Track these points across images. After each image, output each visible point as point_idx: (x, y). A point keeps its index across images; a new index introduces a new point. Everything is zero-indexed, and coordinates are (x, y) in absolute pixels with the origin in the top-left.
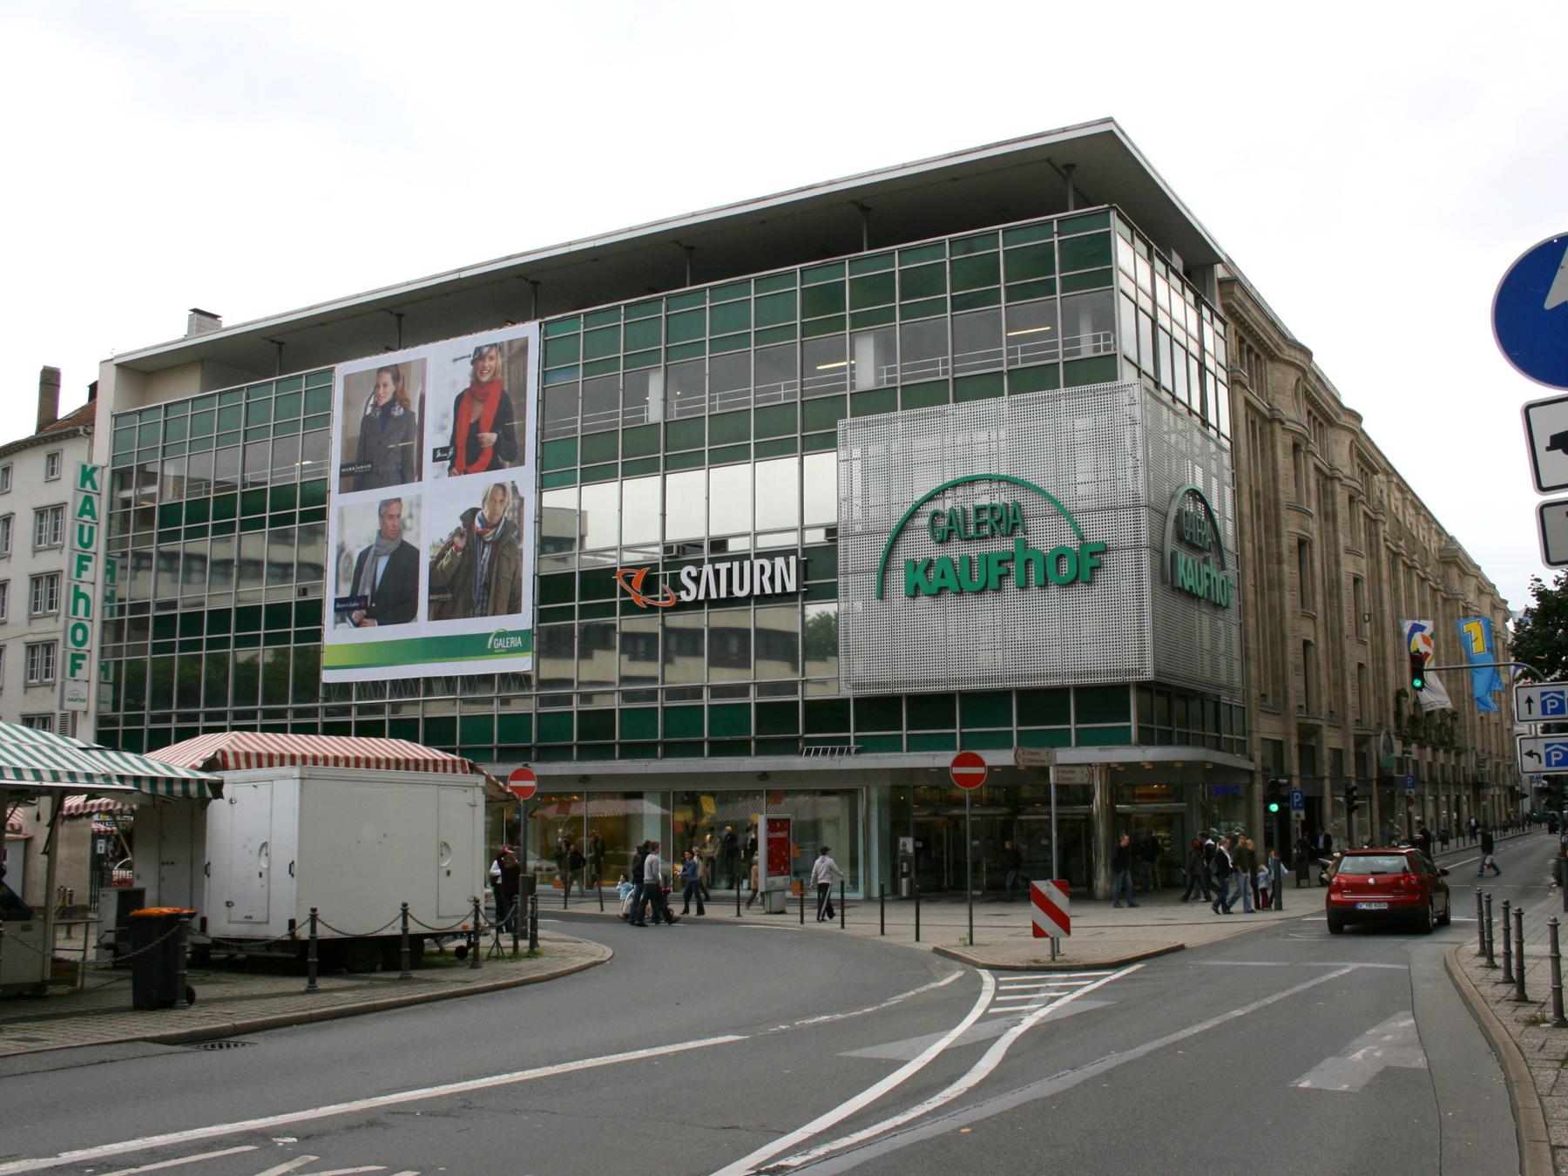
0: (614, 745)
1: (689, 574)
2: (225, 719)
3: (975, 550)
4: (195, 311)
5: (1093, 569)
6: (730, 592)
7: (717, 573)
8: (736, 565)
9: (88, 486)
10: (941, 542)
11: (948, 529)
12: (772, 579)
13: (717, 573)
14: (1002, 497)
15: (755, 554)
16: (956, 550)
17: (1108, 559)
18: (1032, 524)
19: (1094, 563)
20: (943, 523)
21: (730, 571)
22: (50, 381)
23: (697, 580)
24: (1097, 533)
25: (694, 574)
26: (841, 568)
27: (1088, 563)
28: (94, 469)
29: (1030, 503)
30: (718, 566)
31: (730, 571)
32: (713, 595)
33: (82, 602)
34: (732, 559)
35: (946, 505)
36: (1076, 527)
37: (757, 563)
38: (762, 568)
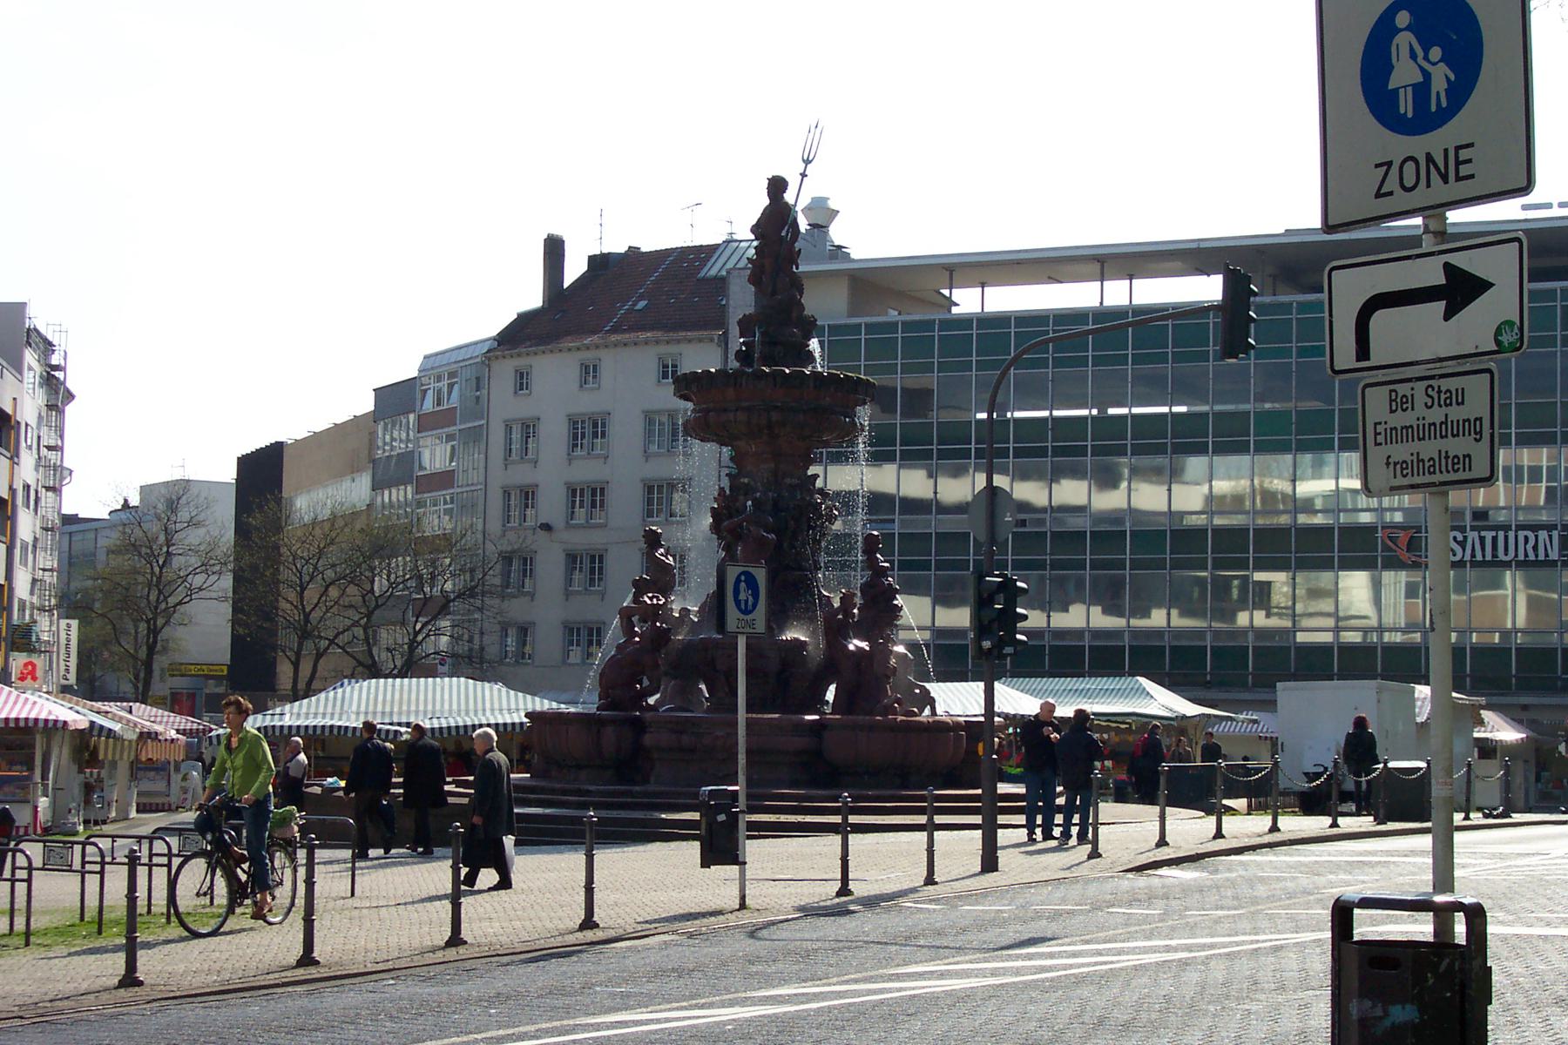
1: (1455, 538)
6: (1494, 555)
7: (1482, 539)
8: (1501, 534)
12: (1535, 548)
13: (1482, 539)
15: (1516, 526)
21: (1495, 539)
22: (554, 249)
23: (1463, 544)
25: (1460, 538)
30: (1483, 533)
31: (1495, 539)
32: (1479, 557)
34: (1496, 528)
37: (1521, 534)
38: (1526, 539)
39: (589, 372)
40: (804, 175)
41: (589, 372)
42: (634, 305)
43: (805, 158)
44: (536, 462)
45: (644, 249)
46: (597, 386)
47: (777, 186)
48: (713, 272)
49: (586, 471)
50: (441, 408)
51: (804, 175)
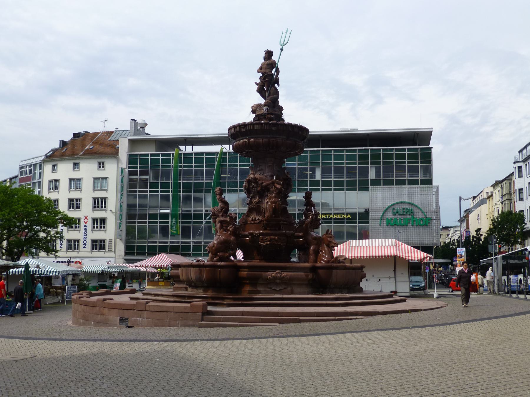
0: (202, 253)
2: (179, 243)
3: (402, 218)
4: (133, 120)
5: (428, 223)
9: (122, 175)
10: (394, 215)
16: (399, 217)
19: (429, 222)
20: (395, 211)
24: (429, 216)
26: (370, 219)
27: (427, 222)
28: (123, 169)
29: (414, 208)
33: (121, 207)
35: (396, 207)
36: (424, 214)
39: (76, 166)
40: (282, 50)
41: (76, 166)
42: (90, 147)
43: (282, 43)
44: (59, 192)
45: (91, 132)
46: (78, 170)
47: (269, 54)
48: (113, 139)
49: (75, 195)
50: (27, 176)
51: (282, 50)
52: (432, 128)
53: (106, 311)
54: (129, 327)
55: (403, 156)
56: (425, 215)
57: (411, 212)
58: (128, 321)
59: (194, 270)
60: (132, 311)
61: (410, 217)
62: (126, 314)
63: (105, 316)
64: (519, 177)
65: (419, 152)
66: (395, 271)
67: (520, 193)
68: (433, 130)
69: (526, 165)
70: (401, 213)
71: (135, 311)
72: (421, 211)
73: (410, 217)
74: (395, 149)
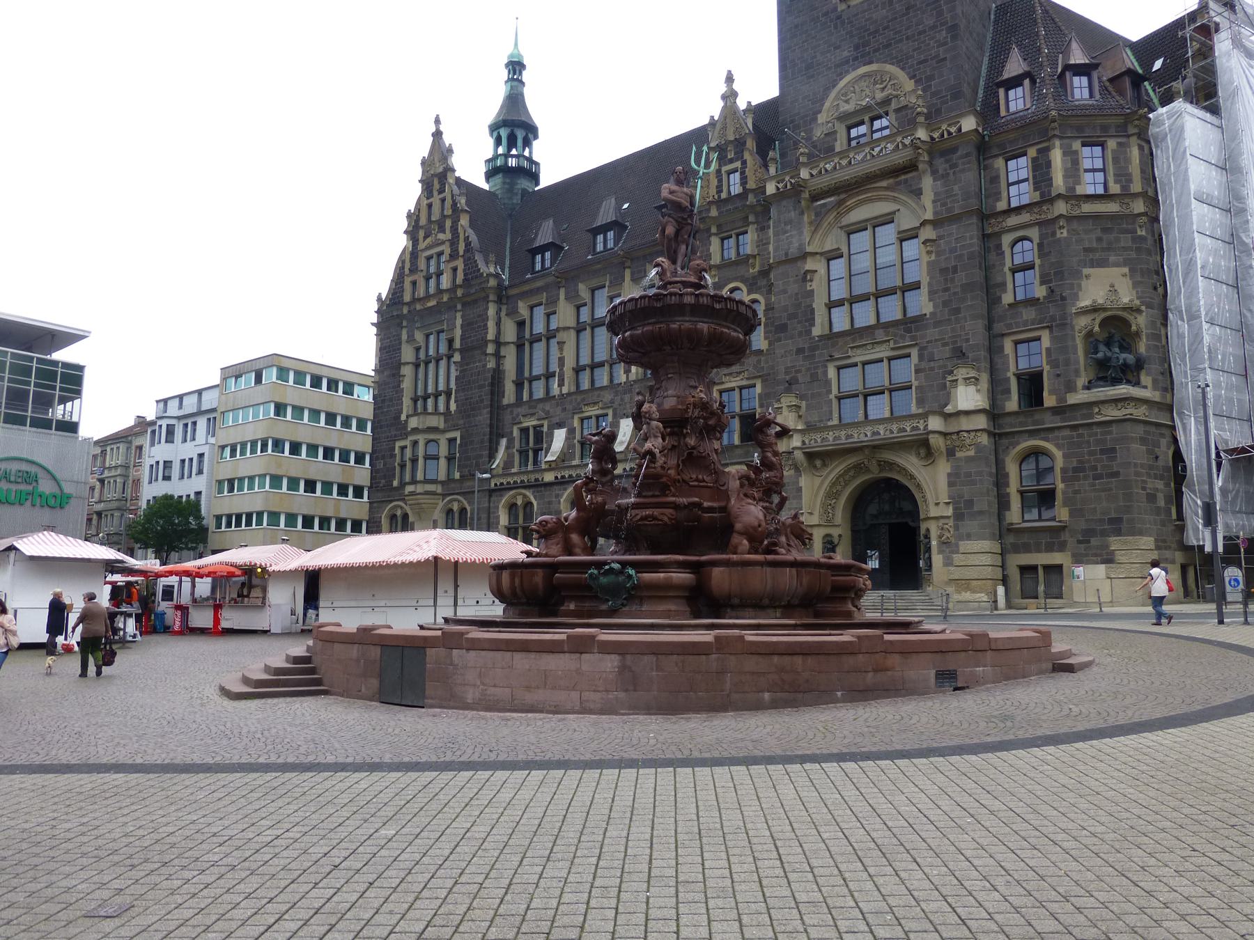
3: (14, 487)
11: (6, 477)
14: (33, 469)
17: (72, 501)
18: (40, 481)
24: (68, 489)
52: (90, 332)
53: (895, 660)
54: (956, 689)
55: (27, 371)
56: (61, 490)
57: (29, 479)
58: (955, 678)
59: (540, 571)
60: (963, 654)
61: (30, 488)
62: (951, 663)
63: (889, 673)
64: (166, 442)
65: (60, 370)
66: (456, 587)
67: (165, 468)
68: (91, 335)
69: (186, 425)
70: (12, 479)
71: (861, 656)
72: (54, 479)
73: (30, 488)
74: (12, 353)
